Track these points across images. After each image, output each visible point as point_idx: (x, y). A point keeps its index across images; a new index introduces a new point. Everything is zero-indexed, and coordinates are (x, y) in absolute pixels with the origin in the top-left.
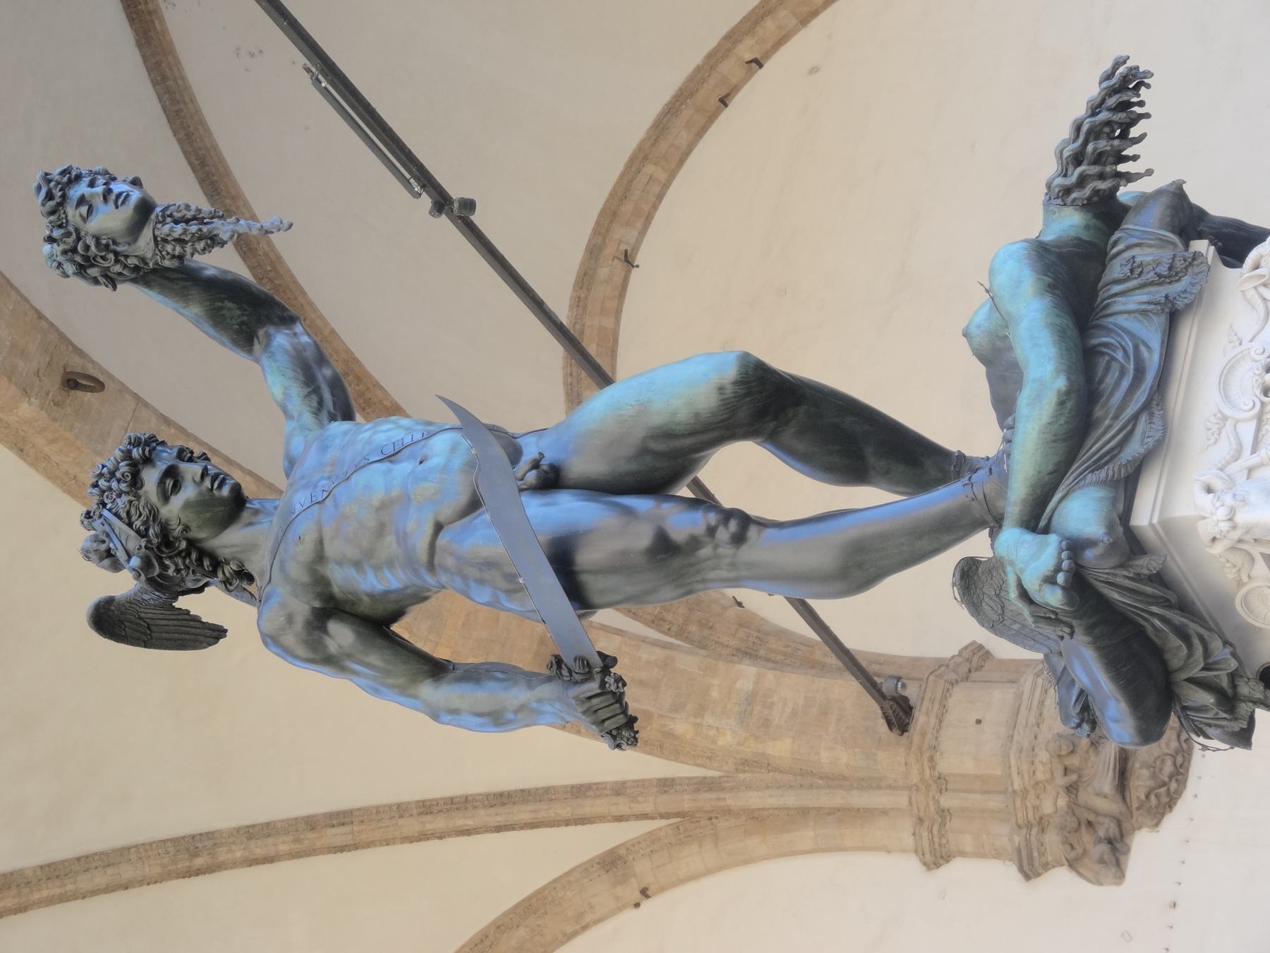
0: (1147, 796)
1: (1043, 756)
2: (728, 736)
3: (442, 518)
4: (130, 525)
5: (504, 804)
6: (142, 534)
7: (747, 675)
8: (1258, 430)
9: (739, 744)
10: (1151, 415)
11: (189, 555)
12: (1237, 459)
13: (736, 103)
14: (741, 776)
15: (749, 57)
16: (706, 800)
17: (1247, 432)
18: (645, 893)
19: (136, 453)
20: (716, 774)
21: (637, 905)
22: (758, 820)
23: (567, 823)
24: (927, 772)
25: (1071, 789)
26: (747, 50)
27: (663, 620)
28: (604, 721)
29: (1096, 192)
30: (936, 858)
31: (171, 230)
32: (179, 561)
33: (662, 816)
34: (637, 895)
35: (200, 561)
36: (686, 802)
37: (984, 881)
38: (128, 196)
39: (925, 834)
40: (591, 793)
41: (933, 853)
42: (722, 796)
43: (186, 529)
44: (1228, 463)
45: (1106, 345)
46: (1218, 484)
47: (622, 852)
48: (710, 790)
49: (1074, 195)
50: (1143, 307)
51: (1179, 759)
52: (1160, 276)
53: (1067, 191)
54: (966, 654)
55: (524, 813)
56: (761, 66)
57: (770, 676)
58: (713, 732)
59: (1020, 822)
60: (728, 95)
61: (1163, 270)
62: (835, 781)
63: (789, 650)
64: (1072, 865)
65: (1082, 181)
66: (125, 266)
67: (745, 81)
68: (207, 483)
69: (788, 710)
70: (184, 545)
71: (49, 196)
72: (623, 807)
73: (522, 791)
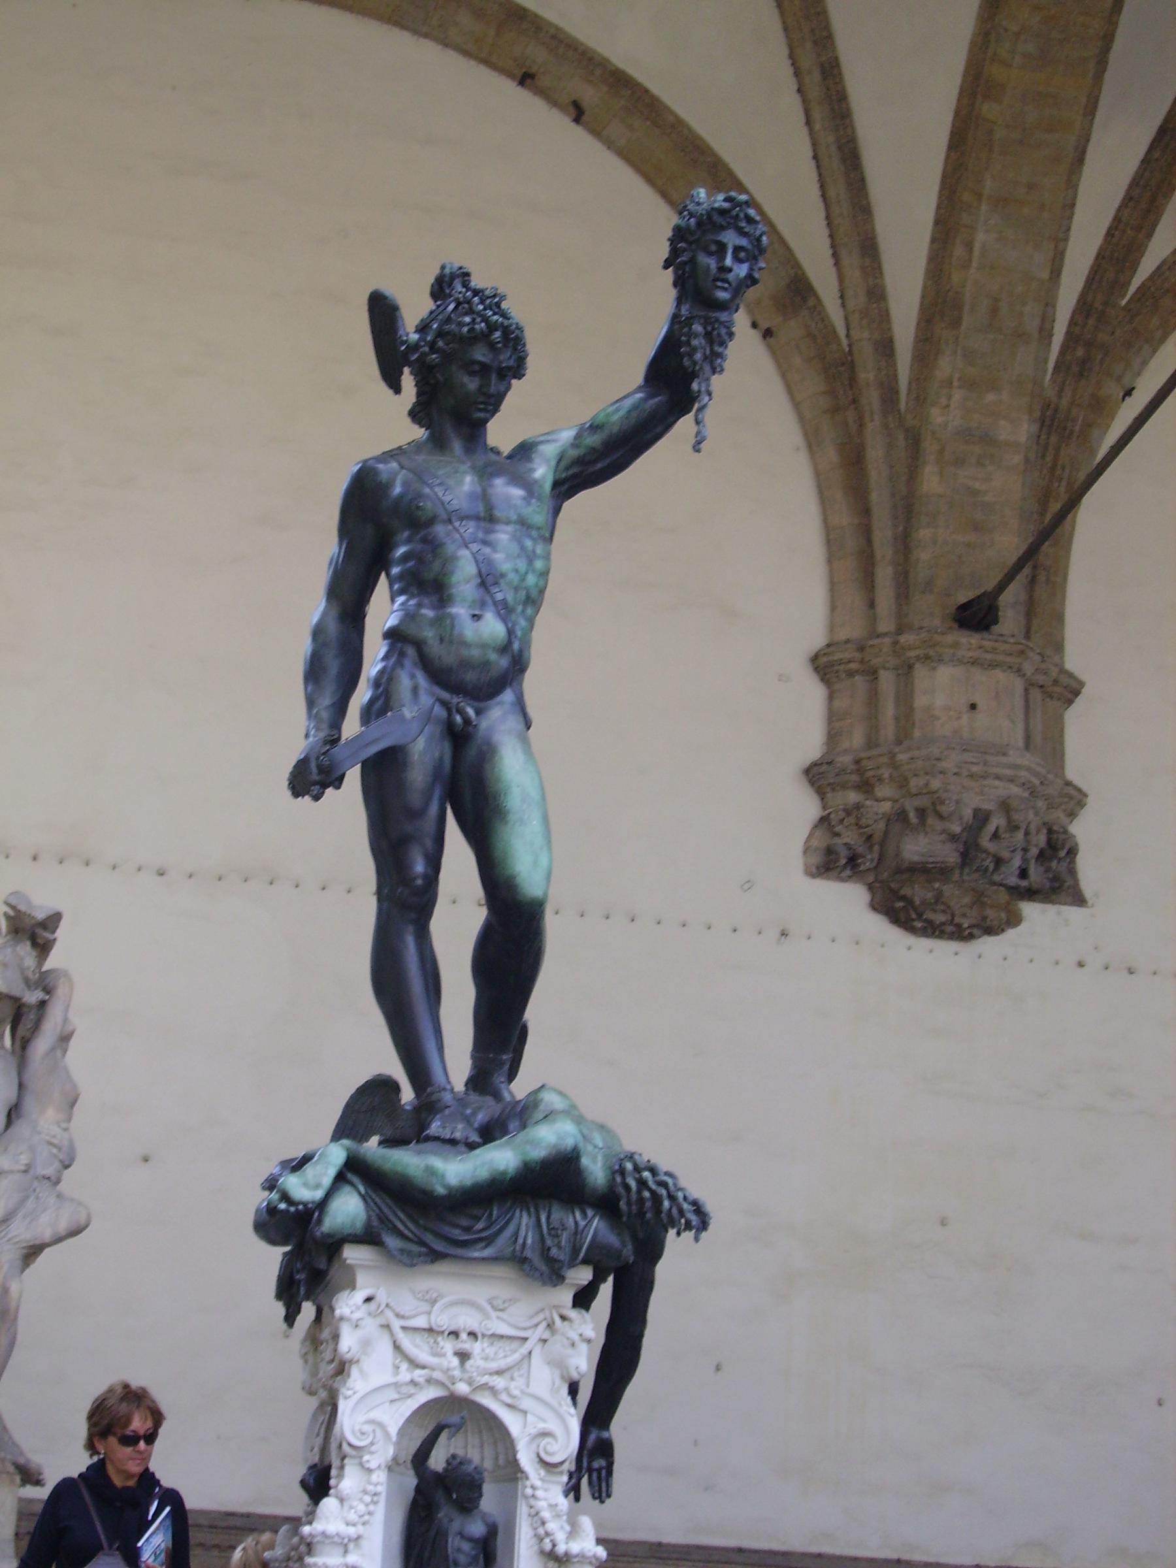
0: (903, 898)
1: (935, 784)
2: (946, 416)
4: (440, 334)
5: (844, 160)
6: (432, 345)
7: (1018, 430)
8: (424, 1330)
9: (933, 433)
10: (426, 1255)
12: (398, 1315)
14: (901, 436)
16: (872, 399)
17: (421, 1322)
18: (768, 334)
19: (497, 334)
20: (903, 405)
21: (754, 325)
22: (854, 461)
23: (831, 236)
24: (913, 654)
25: (902, 816)
27: (1088, 316)
29: (617, 1198)
30: (823, 665)
31: (696, 336)
33: (850, 346)
34: (764, 325)
36: (867, 374)
37: (801, 720)
39: (847, 655)
40: (867, 261)
41: (831, 665)
42: (876, 417)
44: (393, 1311)
45: (491, 1214)
46: (372, 1306)
47: (811, 302)
48: (884, 401)
49: (618, 1179)
50: (520, 1241)
51: (950, 929)
52: (549, 1249)
53: (622, 1172)
54: (1064, 680)
55: (838, 189)
57: (1017, 459)
58: (944, 401)
59: (864, 763)
61: (554, 1252)
62: (904, 544)
63: (1058, 472)
64: (824, 820)
65: (627, 1187)
68: (481, 399)
69: (977, 485)
71: (722, 212)
72: (858, 299)
73: (863, 180)
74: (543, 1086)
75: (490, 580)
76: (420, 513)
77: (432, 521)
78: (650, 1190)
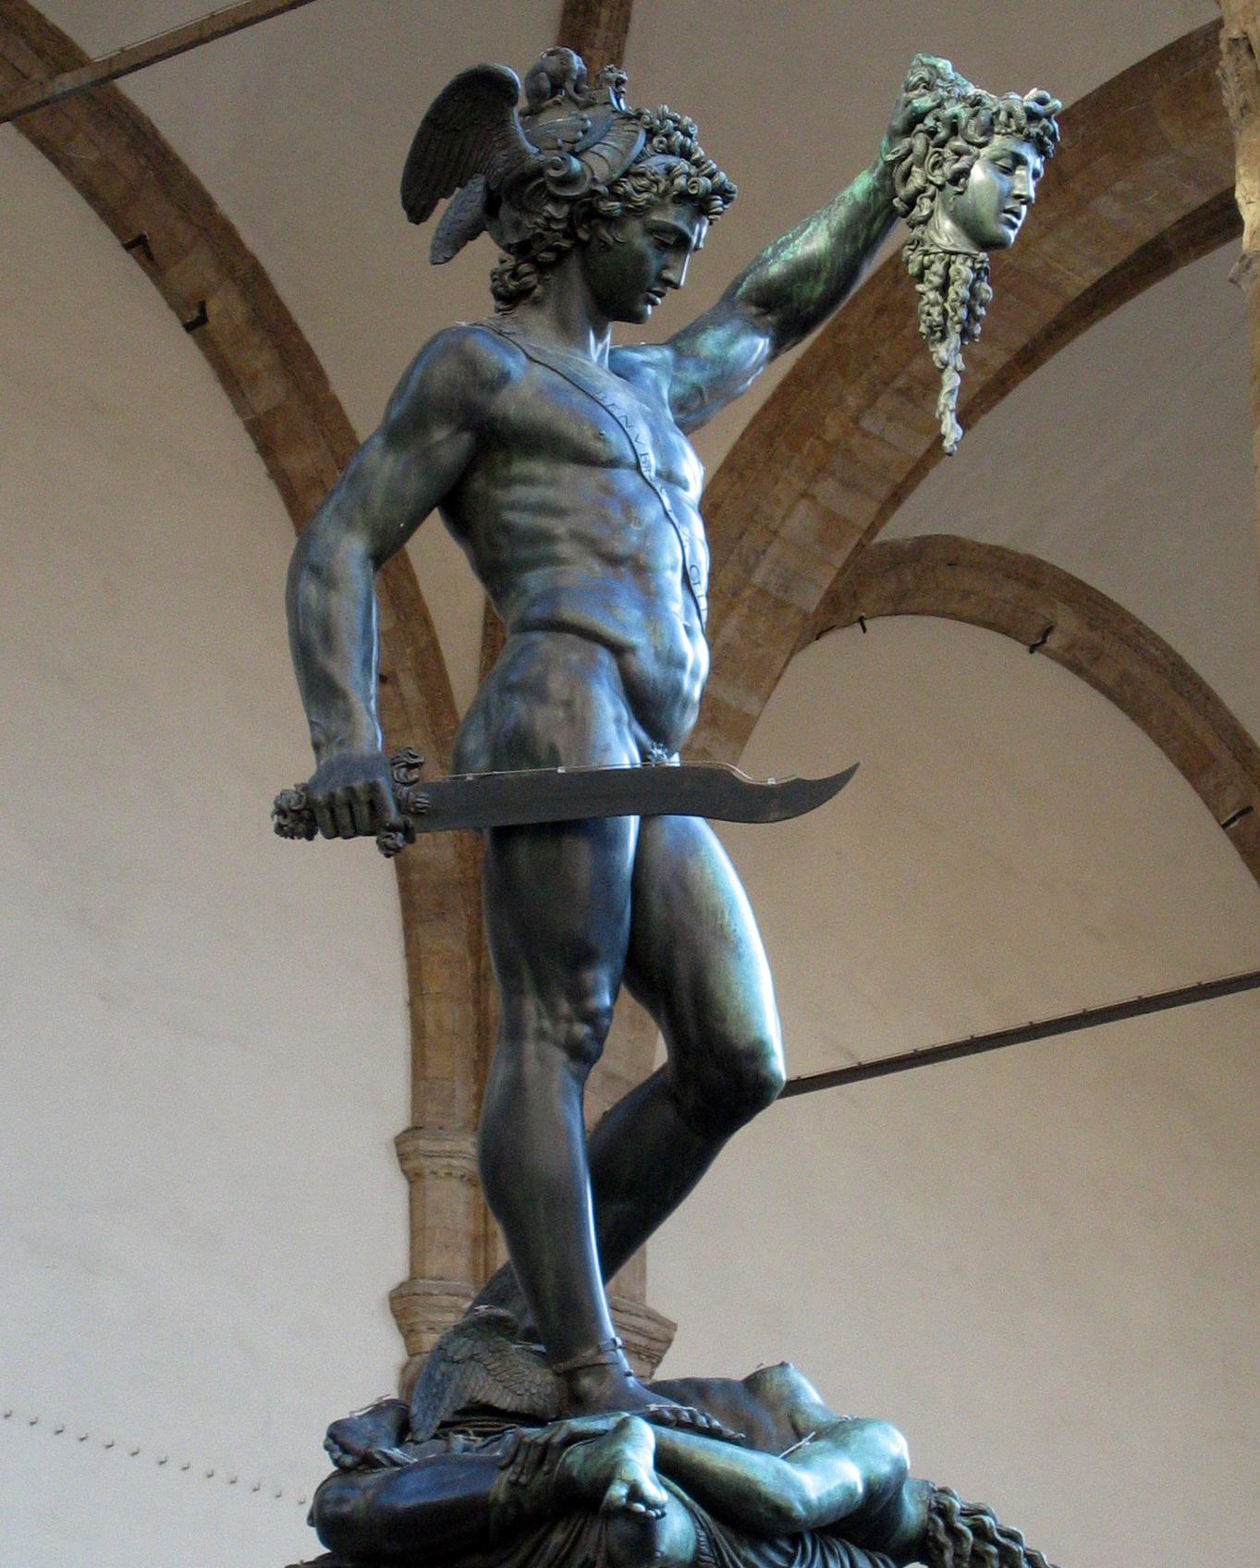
3: (629, 657)
4: (626, 174)
6: (613, 184)
11: (566, 235)
13: (127, 264)
15: (213, 307)
26: (226, 307)
28: (332, 811)
29: (941, 1549)
32: (561, 226)
35: (557, 249)
38: (1013, 226)
43: (607, 248)
49: (940, 1522)
53: (944, 1512)
56: (189, 327)
60: (150, 256)
66: (920, 191)
67: (167, 293)
70: (583, 236)
74: (783, 1365)
75: (692, 573)
76: (599, 445)
77: (614, 463)
78: (996, 1543)
